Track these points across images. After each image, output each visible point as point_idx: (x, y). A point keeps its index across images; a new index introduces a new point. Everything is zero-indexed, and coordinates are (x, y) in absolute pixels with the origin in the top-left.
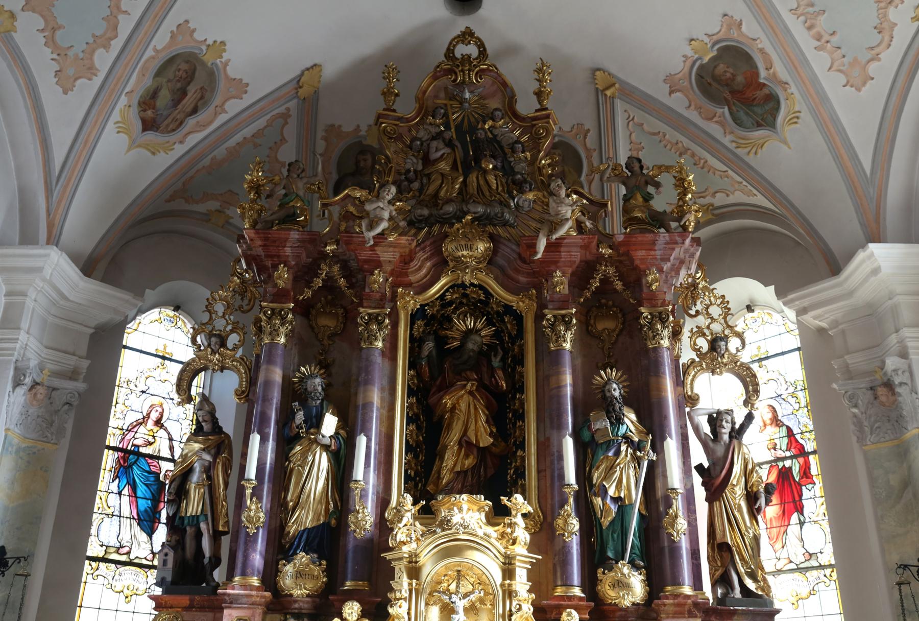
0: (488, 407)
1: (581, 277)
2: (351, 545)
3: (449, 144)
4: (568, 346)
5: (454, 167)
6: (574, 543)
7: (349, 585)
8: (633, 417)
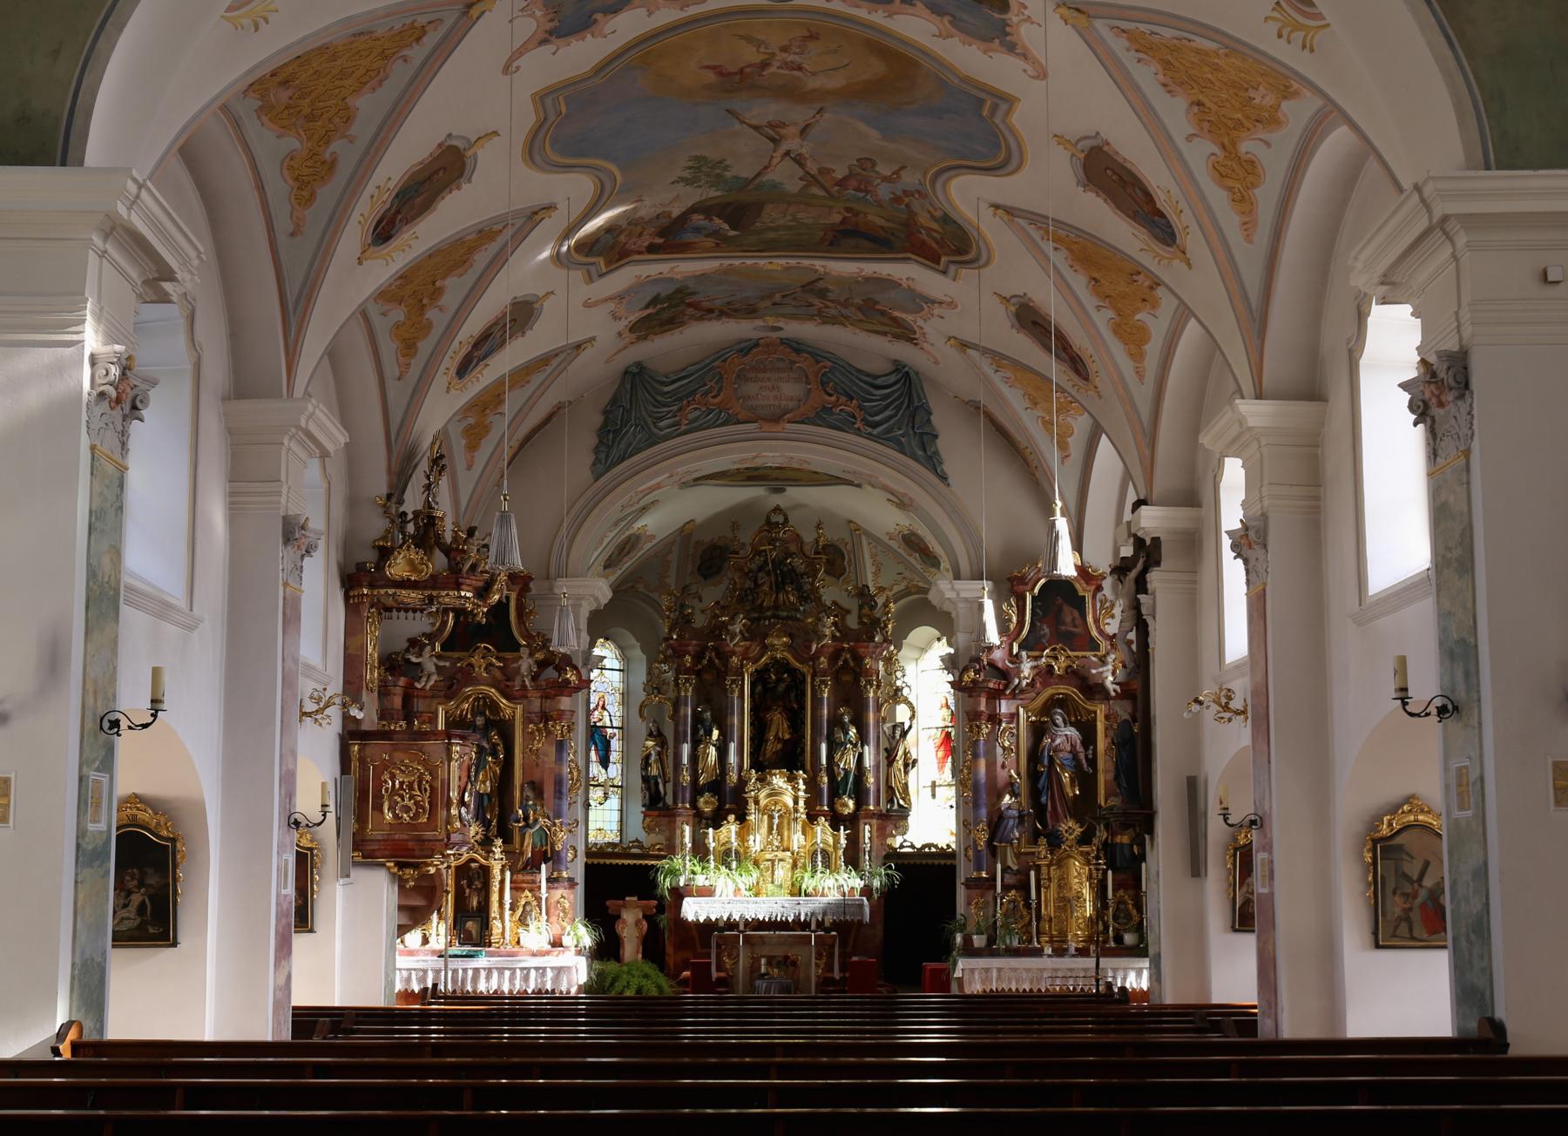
0: (788, 719)
1: (834, 657)
2: (728, 789)
3: (768, 574)
4: (826, 695)
5: (771, 588)
6: (825, 787)
7: (727, 806)
8: (855, 731)
